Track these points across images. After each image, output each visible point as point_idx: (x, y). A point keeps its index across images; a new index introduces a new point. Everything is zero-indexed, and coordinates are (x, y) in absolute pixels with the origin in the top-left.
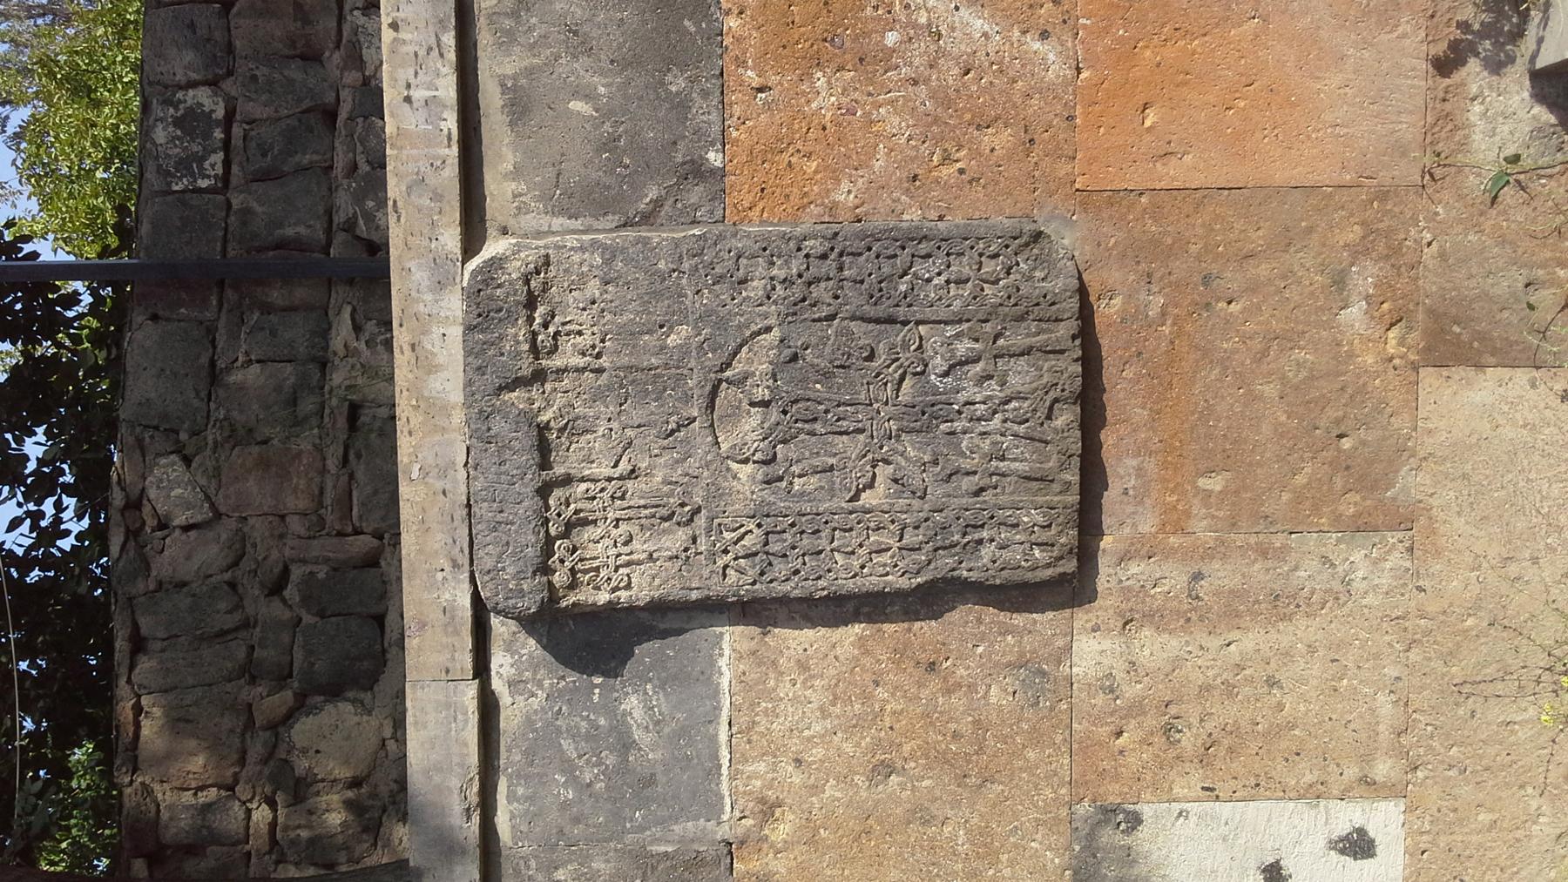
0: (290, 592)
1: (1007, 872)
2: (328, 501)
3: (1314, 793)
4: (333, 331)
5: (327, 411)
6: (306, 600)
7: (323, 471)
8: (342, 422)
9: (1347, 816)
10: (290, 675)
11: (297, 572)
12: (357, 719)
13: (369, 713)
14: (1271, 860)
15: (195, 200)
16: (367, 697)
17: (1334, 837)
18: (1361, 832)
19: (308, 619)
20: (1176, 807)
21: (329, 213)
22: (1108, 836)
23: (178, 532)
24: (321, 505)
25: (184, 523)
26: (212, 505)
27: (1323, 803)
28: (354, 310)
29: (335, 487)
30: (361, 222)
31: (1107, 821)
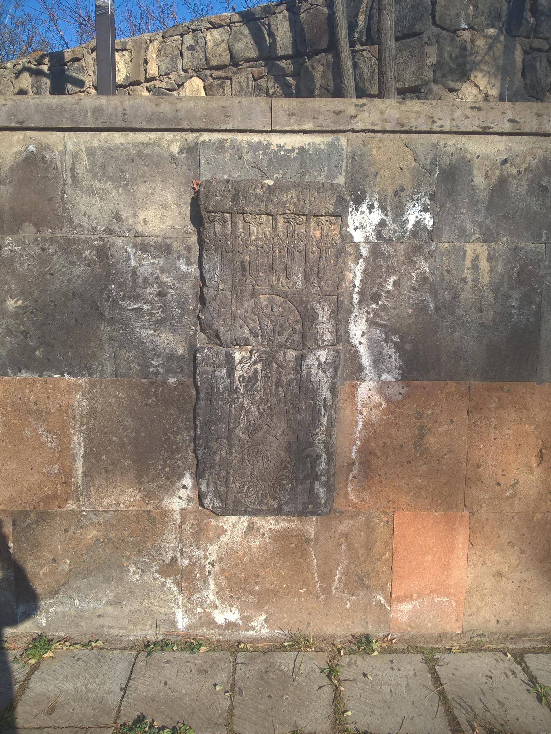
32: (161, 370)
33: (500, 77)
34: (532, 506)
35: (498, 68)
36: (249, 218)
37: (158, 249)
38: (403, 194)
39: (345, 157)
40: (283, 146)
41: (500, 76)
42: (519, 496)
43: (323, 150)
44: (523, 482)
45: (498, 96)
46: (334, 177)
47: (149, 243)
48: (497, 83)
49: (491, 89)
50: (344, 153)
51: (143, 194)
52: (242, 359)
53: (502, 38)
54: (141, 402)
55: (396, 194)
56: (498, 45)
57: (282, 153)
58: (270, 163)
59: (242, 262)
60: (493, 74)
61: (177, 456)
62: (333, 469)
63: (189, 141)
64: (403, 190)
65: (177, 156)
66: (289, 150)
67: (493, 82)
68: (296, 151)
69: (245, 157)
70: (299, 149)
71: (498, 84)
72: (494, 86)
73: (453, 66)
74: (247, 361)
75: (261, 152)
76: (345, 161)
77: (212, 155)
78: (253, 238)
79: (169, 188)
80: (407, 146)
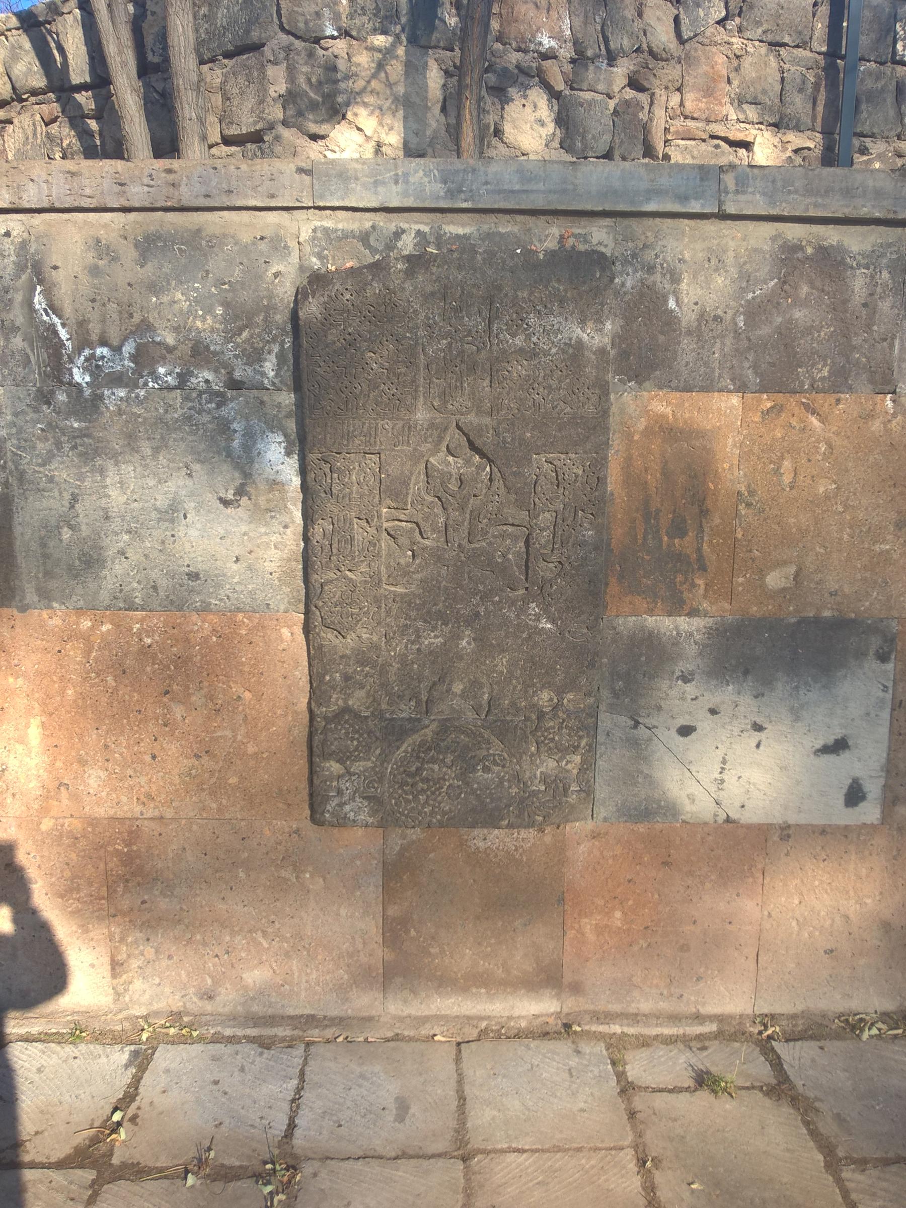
0: (630, 94)
1: (859, 576)
2: (690, 123)
3: (891, 769)
4: (799, 134)
5: (748, 126)
6: (627, 103)
7: (708, 121)
8: (740, 136)
9: (873, 789)
10: (572, 89)
11: (643, 98)
12: (544, 136)
13: (547, 145)
14: (850, 743)
15: (890, 40)
16: (556, 144)
17: (861, 781)
18: (863, 798)
19: (612, 104)
20: (890, 684)
21: (872, 136)
22: (875, 642)
23: (676, 12)
24: (686, 117)
25: (681, 16)
26: (690, 39)
27: (884, 774)
28: (809, 149)
29: (697, 128)
30: (865, 158)
31: (885, 641)
33: (401, 113)
34: (36, 807)
35: (396, 99)
41: (401, 112)
42: (11, 791)
44: (16, 768)
45: (401, 146)
48: (396, 125)
49: (387, 134)
53: (401, 51)
56: (394, 62)
60: (389, 108)
67: (389, 122)
71: (399, 125)
72: (391, 129)
73: (317, 97)
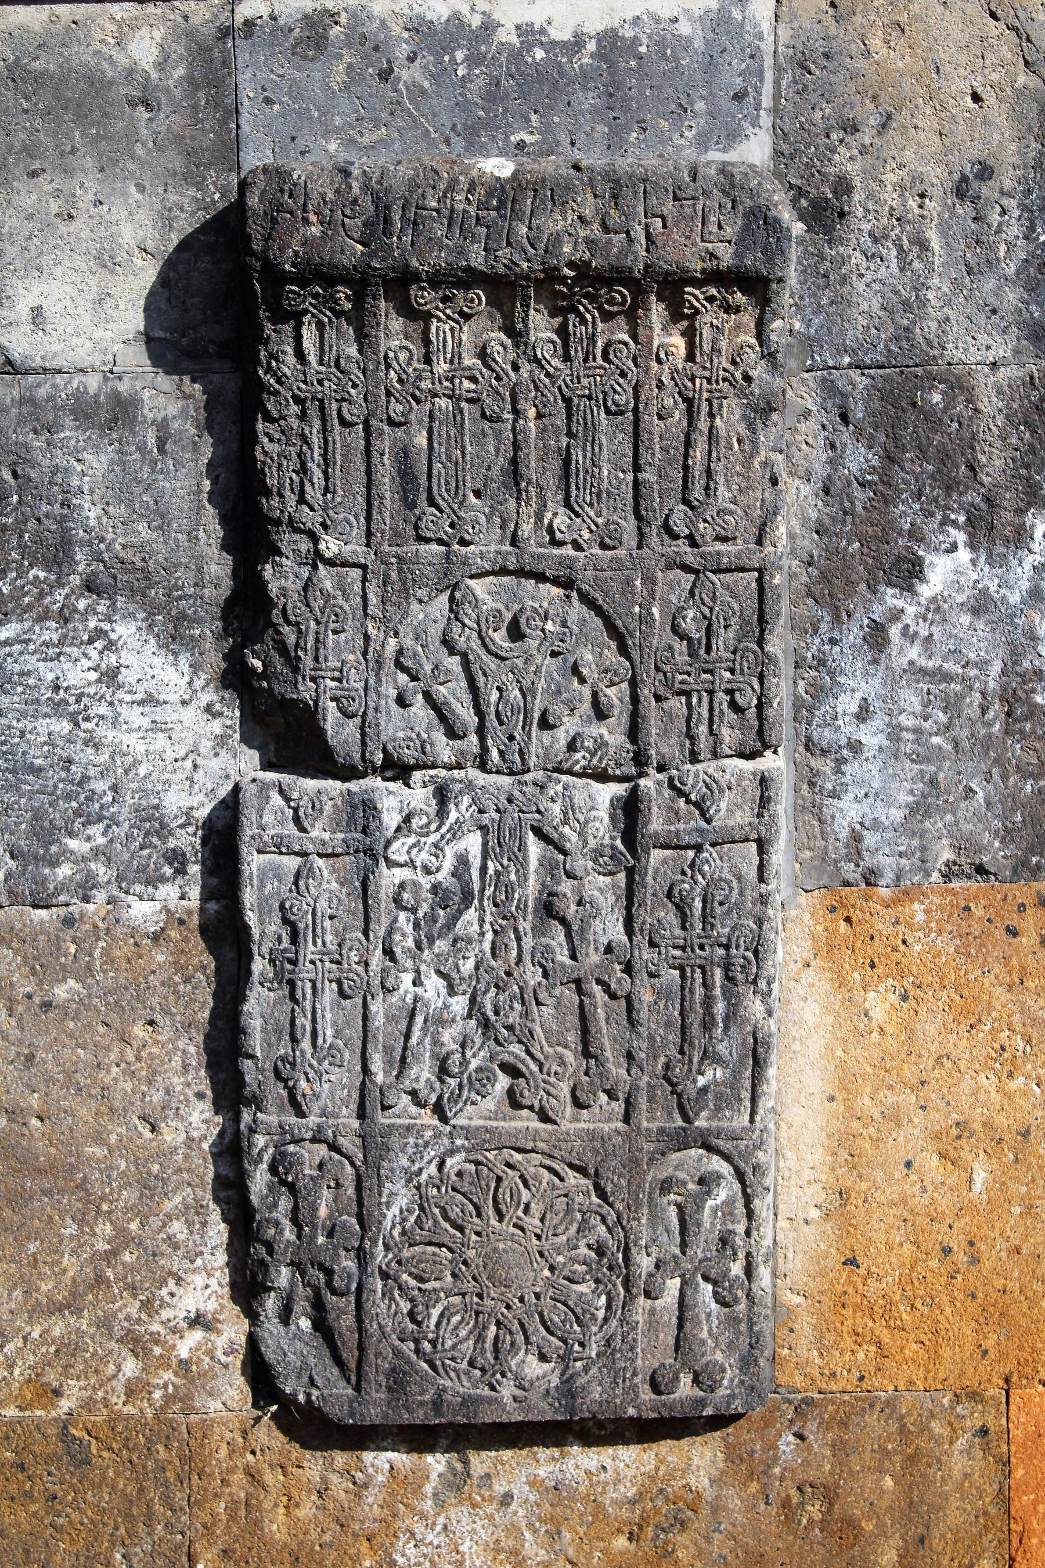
32: (101, 871)
36: (425, 298)
37: (88, 416)
38: (987, 190)
39: (768, 62)
40: (543, 31)
43: (689, 40)
46: (733, 136)
47: (50, 398)
50: (767, 46)
51: (29, 217)
52: (407, 819)
54: (29, 996)
55: (961, 190)
57: (540, 54)
58: (493, 94)
59: (404, 456)
61: (168, 1206)
62: (767, 1231)
63: (196, 20)
64: (985, 172)
65: (154, 76)
66: (564, 45)
68: (591, 46)
69: (405, 74)
70: (600, 38)
74: (428, 825)
75: (460, 56)
76: (769, 76)
77: (283, 68)
78: (441, 367)
79: (125, 195)
80: (993, 15)
